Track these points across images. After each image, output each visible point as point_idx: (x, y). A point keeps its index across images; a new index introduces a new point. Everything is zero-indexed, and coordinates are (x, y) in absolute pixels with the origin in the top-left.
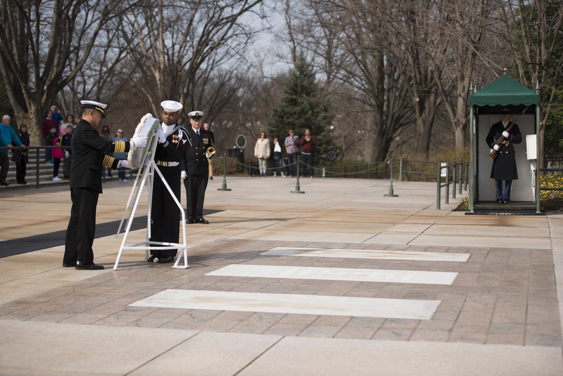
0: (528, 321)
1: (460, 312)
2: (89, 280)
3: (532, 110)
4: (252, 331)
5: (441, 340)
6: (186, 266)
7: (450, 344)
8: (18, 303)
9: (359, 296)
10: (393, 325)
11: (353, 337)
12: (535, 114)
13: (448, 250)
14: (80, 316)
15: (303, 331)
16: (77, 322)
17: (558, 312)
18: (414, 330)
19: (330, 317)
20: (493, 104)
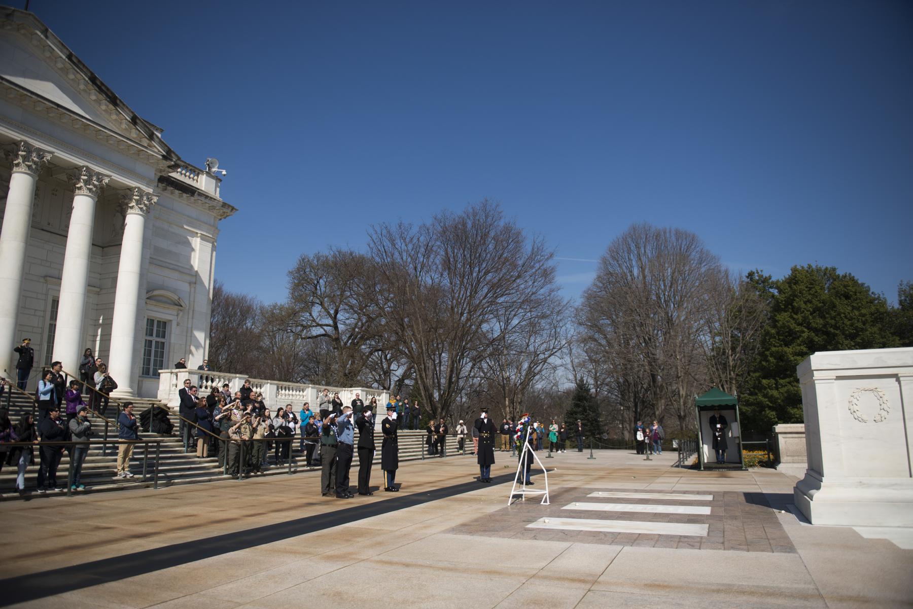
0: (769, 537)
1: (724, 531)
2: (496, 512)
3: (733, 407)
4: (604, 543)
5: (720, 549)
6: (548, 503)
7: (726, 552)
8: (463, 525)
9: (658, 522)
10: (686, 539)
11: (665, 547)
12: (736, 410)
13: (698, 493)
14: (501, 533)
15: (633, 543)
16: (500, 537)
17: (785, 531)
18: (701, 543)
19: (646, 534)
20: (709, 404)
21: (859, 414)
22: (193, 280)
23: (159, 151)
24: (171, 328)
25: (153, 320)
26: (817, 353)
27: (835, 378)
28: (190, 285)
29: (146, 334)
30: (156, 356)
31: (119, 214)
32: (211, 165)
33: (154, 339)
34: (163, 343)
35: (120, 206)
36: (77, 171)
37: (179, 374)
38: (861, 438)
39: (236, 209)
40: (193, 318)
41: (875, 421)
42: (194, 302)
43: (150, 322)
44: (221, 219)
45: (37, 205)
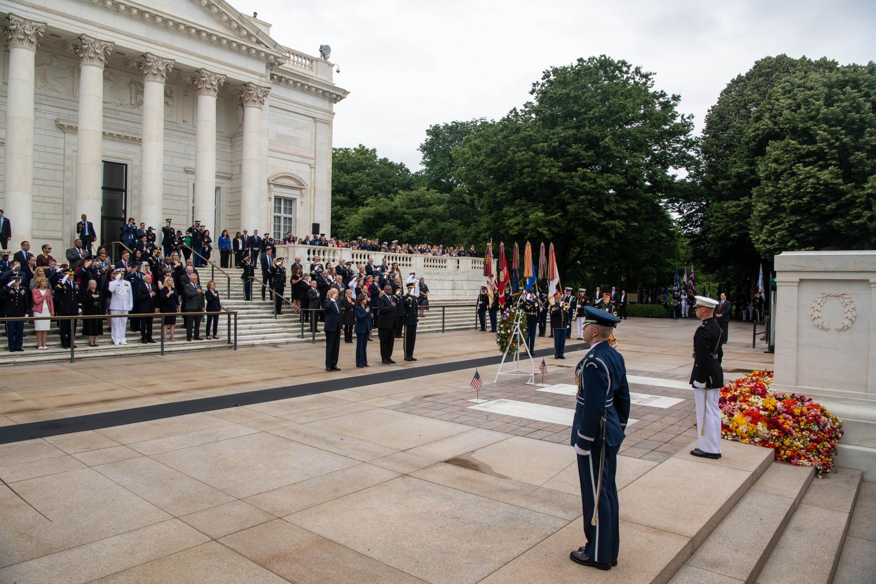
21: (820, 321)
22: (312, 162)
23: (267, 47)
24: (296, 204)
25: (281, 199)
26: (784, 254)
27: (799, 281)
28: (311, 168)
29: (275, 212)
30: (285, 230)
31: (240, 107)
32: (324, 51)
33: (283, 215)
34: (290, 219)
35: (241, 99)
36: (198, 74)
38: (819, 347)
39: (349, 93)
40: (314, 196)
41: (837, 329)
42: (315, 181)
43: (278, 199)
44: (336, 103)
45: (172, 106)
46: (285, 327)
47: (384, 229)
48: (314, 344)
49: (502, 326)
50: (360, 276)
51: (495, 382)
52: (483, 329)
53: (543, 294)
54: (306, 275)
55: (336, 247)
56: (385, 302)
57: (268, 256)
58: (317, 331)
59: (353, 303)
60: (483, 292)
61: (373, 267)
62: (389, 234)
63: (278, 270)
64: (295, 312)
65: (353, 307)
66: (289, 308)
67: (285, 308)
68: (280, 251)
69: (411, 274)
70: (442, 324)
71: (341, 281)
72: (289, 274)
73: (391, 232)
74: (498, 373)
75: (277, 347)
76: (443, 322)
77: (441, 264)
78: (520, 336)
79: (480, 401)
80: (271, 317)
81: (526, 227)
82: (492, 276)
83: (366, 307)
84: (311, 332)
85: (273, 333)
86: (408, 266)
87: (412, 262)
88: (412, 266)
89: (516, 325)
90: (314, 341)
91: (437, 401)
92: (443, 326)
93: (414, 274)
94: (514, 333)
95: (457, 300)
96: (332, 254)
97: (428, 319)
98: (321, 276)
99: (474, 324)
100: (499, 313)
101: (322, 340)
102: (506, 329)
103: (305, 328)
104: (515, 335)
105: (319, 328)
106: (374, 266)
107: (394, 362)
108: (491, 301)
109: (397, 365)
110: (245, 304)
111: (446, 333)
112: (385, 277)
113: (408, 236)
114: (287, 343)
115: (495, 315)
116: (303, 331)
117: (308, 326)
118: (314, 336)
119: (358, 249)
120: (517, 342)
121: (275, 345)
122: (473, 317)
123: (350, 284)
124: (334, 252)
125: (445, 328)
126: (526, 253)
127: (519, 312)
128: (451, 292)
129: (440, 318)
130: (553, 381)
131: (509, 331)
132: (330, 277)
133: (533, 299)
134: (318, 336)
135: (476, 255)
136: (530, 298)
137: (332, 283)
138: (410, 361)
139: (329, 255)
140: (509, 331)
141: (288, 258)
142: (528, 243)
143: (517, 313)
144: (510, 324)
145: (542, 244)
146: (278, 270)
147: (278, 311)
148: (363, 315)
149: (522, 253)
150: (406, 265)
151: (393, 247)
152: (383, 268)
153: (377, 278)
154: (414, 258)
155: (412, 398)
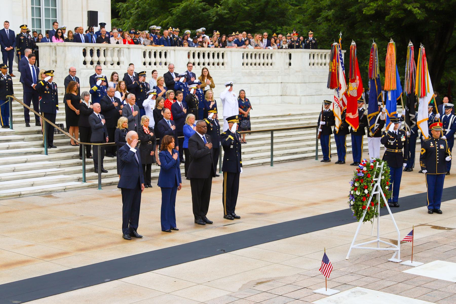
30: (47, 15)
37: (57, 48)
46: (60, 166)
47: (183, 5)
48: (101, 190)
49: (356, 184)
50: (159, 91)
51: (347, 258)
52: (326, 158)
53: (411, 115)
54: (85, 94)
55: (121, 45)
56: (198, 144)
57: (30, 65)
58: (103, 171)
59: (152, 134)
60: (326, 108)
61: (174, 76)
62: (191, 10)
63: (47, 88)
64: (72, 143)
65: (152, 139)
66: (64, 137)
67: (58, 138)
68: (43, 48)
69: (227, 85)
70: (269, 153)
71: (134, 102)
72: (61, 92)
73: (194, 9)
74: (352, 246)
75: (51, 196)
76: (272, 150)
77: (266, 61)
78: (381, 196)
79: (330, 291)
80: (40, 153)
81: (389, 4)
82: (340, 88)
83: (173, 152)
84: (96, 171)
85: (45, 176)
86: (221, 65)
87: (226, 60)
88: (225, 65)
89: (376, 182)
90: (100, 185)
91: (273, 291)
92: (272, 156)
93: (231, 85)
94: (373, 193)
95: (289, 115)
96: (116, 53)
97: (251, 146)
98: (106, 94)
99: (313, 151)
100: (349, 138)
101: (111, 184)
102: (362, 189)
103: (88, 167)
104: (375, 195)
105: (105, 165)
106: (176, 75)
107: (211, 223)
108: (338, 122)
109: (216, 227)
110: (4, 134)
111: (275, 166)
112: (192, 92)
113: (217, 14)
114: (65, 190)
115: (344, 141)
116: (85, 171)
117: (90, 163)
118: (100, 178)
119: (151, 44)
120: (377, 203)
121: (48, 194)
122: (312, 140)
123: (145, 103)
124: (119, 51)
125: (275, 159)
126: (388, 56)
127: (380, 164)
128: (279, 98)
129: (267, 144)
130: (427, 255)
131: (366, 191)
132: (118, 95)
133: (399, 131)
134: (105, 177)
135: (315, 46)
136: (395, 129)
137: (120, 103)
138: (232, 219)
139: (112, 56)
140: (366, 191)
141: (56, 62)
142: (392, 42)
143: (378, 166)
144: (368, 182)
145: (411, 44)
146: (47, 88)
147: (50, 143)
148: (170, 164)
149: (383, 58)
150: (218, 64)
151: (200, 39)
152: (189, 77)
153: (181, 96)
154: (229, 53)
155: (240, 286)
